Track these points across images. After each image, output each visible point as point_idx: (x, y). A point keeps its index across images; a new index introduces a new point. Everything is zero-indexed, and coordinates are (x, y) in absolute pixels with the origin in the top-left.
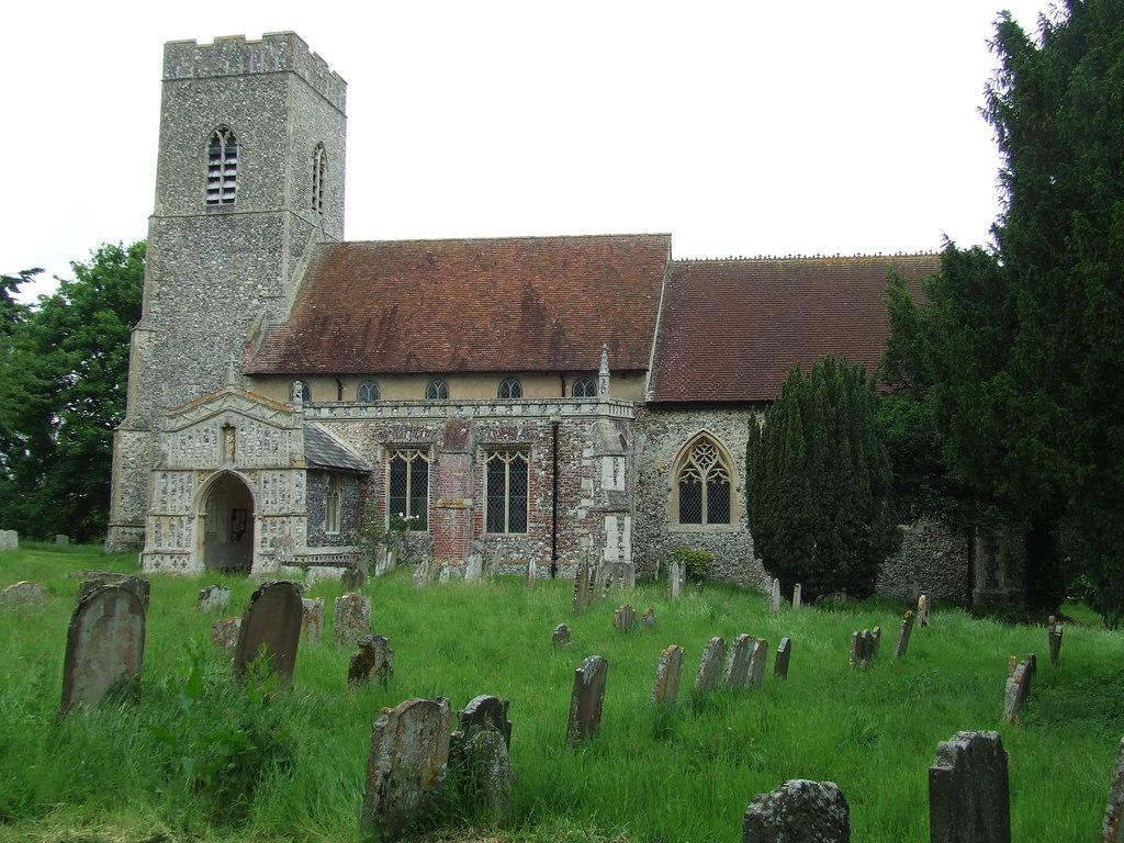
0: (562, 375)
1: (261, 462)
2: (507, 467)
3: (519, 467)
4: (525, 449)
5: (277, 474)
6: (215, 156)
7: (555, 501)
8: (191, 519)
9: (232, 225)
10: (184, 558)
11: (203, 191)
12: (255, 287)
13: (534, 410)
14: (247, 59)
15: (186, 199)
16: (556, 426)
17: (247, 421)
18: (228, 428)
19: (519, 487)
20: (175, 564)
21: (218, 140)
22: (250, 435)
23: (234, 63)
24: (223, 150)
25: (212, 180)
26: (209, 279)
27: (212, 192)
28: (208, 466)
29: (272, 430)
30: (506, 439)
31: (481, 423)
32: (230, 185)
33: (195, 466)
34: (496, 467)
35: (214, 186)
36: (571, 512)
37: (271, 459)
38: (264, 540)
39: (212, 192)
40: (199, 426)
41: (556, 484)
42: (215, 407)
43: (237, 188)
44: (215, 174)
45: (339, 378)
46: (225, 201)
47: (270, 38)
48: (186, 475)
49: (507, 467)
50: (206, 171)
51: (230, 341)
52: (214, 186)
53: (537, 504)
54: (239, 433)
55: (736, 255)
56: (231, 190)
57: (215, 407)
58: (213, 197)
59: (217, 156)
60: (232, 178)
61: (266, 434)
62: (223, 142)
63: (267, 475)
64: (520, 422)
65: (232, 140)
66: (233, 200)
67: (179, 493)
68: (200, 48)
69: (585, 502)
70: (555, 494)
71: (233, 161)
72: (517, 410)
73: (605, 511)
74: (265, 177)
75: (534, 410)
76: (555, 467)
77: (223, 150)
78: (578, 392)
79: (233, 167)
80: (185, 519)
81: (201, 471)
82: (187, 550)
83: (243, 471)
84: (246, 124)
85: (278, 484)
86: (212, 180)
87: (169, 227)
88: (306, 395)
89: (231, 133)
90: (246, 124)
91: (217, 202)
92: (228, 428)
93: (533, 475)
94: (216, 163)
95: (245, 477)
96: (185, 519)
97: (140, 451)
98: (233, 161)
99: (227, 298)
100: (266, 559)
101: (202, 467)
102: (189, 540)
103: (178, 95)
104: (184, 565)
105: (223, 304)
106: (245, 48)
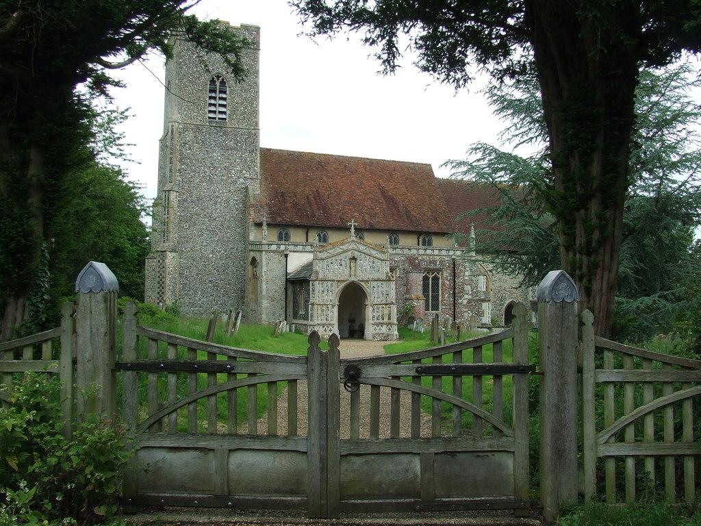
0: (419, 234)
1: (371, 276)
2: (430, 279)
3: (436, 279)
5: (379, 283)
7: (454, 297)
8: (333, 306)
9: (225, 134)
12: (241, 171)
15: (196, 114)
18: (354, 259)
19: (435, 290)
21: (215, 82)
22: (364, 263)
24: (218, 88)
25: (210, 105)
26: (212, 164)
27: (210, 112)
29: (376, 260)
30: (432, 266)
31: (420, 258)
32: (223, 109)
33: (335, 278)
34: (425, 279)
35: (213, 108)
36: (460, 301)
37: (376, 276)
39: (210, 112)
40: (336, 257)
41: (455, 288)
42: (345, 247)
43: (228, 112)
45: (307, 228)
46: (219, 119)
47: (245, 28)
48: (329, 283)
49: (430, 279)
50: (207, 99)
51: (227, 201)
52: (213, 108)
53: (445, 297)
54: (358, 261)
56: (225, 113)
57: (345, 247)
58: (212, 115)
59: (215, 91)
62: (218, 84)
63: (375, 284)
64: (438, 258)
65: (223, 83)
66: (225, 119)
69: (466, 296)
70: (454, 293)
71: (224, 96)
72: (429, 252)
73: (484, 301)
74: (245, 108)
75: (444, 253)
76: (454, 282)
77: (218, 88)
78: (424, 244)
79: (225, 99)
80: (330, 307)
81: (338, 281)
82: (332, 322)
83: (362, 281)
85: (380, 289)
86: (210, 105)
87: (185, 130)
89: (223, 79)
91: (215, 118)
92: (354, 259)
94: (213, 95)
95: (362, 283)
96: (330, 307)
98: (224, 96)
99: (224, 176)
100: (375, 326)
101: (339, 279)
102: (332, 317)
105: (222, 180)
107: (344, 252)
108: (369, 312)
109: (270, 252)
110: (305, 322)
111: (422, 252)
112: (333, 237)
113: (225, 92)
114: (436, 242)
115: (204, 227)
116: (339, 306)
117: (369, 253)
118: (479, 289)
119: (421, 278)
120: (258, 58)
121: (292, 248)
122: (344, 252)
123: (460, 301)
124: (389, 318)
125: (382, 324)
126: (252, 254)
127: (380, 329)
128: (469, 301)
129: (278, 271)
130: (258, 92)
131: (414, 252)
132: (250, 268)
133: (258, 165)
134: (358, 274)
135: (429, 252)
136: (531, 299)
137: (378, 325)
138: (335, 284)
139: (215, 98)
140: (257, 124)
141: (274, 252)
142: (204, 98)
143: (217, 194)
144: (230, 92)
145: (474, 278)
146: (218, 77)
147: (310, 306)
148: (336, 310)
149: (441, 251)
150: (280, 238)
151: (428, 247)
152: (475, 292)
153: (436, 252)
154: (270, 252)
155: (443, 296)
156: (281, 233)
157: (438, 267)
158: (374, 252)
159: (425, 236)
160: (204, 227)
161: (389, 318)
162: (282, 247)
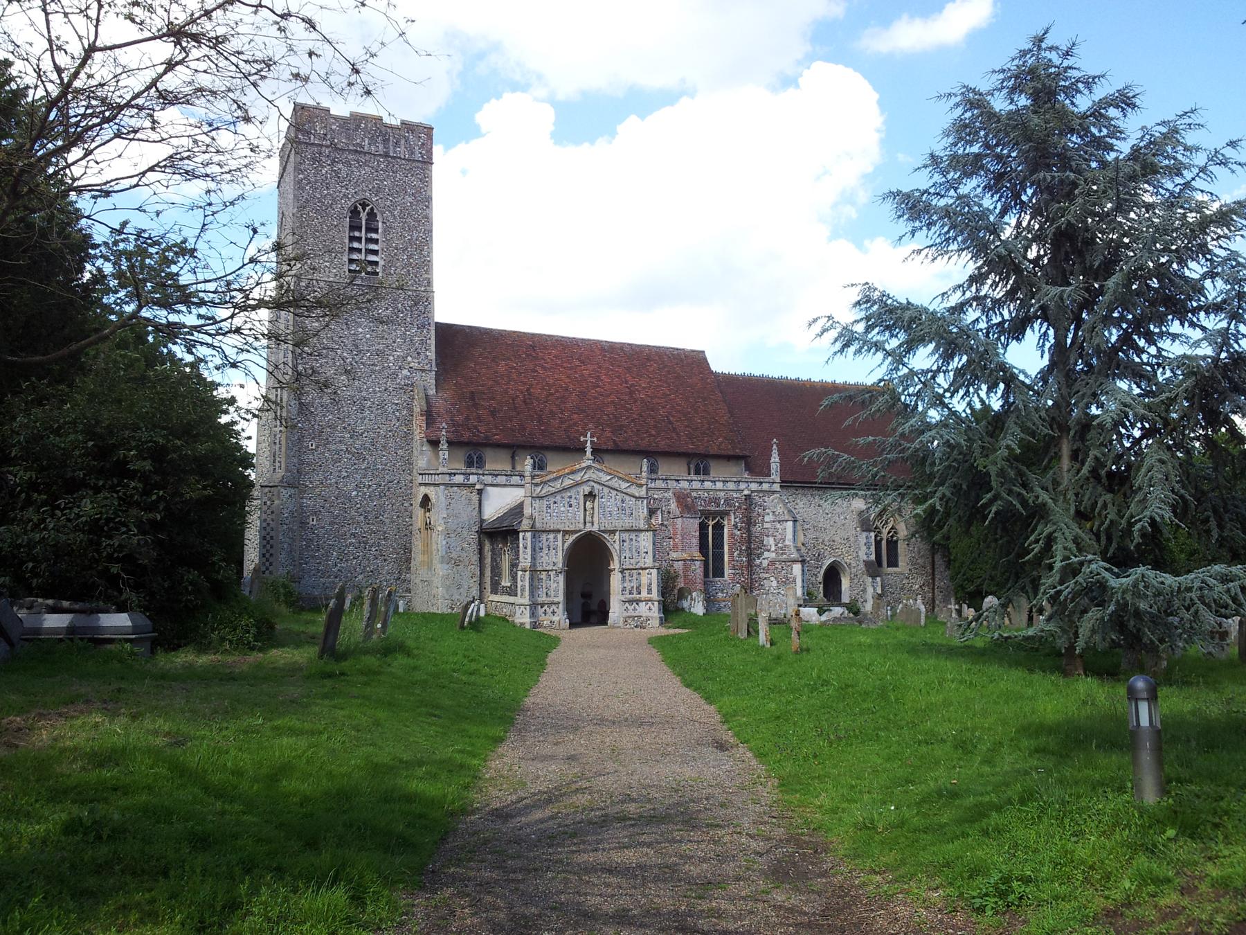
0: (686, 456)
1: (619, 524)
3: (719, 528)
4: (724, 514)
5: (633, 536)
6: (354, 227)
10: (554, 607)
11: (346, 259)
12: (404, 358)
13: (731, 486)
14: (386, 141)
16: (748, 497)
17: (606, 490)
18: (591, 496)
19: (718, 544)
20: (545, 613)
22: (609, 502)
23: (373, 141)
25: (352, 250)
28: (572, 528)
30: (713, 508)
31: (694, 494)
33: (561, 527)
34: (703, 527)
36: (758, 562)
37: (628, 522)
38: (624, 589)
41: (749, 542)
42: (578, 477)
43: (381, 263)
44: (356, 245)
45: (514, 449)
47: (408, 126)
48: (551, 536)
50: (347, 241)
55: (747, 372)
57: (578, 477)
60: (375, 252)
61: (623, 501)
62: (363, 216)
63: (626, 536)
64: (722, 494)
65: (372, 215)
67: (545, 551)
68: (336, 118)
69: (766, 554)
70: (749, 548)
71: (374, 236)
72: (708, 485)
73: (794, 561)
74: (410, 257)
75: (731, 486)
76: (749, 531)
78: (697, 473)
79: (376, 241)
81: (566, 532)
82: (556, 600)
84: (388, 203)
86: (352, 250)
88: (653, 470)
89: (372, 209)
90: (388, 203)
93: (732, 536)
94: (357, 234)
97: (291, 507)
98: (374, 236)
102: (556, 591)
103: (314, 159)
104: (554, 613)
105: (373, 371)
106: (383, 129)
107: (578, 484)
108: (615, 581)
109: (452, 485)
110: (512, 599)
111: (696, 485)
112: (555, 464)
113: (376, 231)
114: (717, 470)
115: (344, 447)
116: (567, 572)
117: (616, 486)
118: (787, 543)
119: (697, 526)
120: (430, 177)
121: (488, 479)
122: (578, 484)
123: (758, 562)
124: (649, 591)
125: (638, 601)
126: (423, 490)
127: (635, 609)
128: (772, 563)
129: (467, 515)
130: (431, 231)
131: (684, 485)
132: (419, 512)
133: (433, 348)
134: (596, 519)
135: (708, 485)
136: (865, 558)
137: (631, 602)
138: (560, 536)
139: (359, 240)
140: (429, 283)
141: (459, 486)
142: (341, 238)
143: (364, 394)
144: (385, 231)
145: (778, 526)
146: (364, 206)
147: (520, 573)
148: (561, 578)
149: (724, 484)
150: (469, 464)
151: (706, 477)
152: (782, 550)
153: (719, 485)
154: (452, 485)
155: (731, 554)
156: (470, 457)
157: (722, 508)
158: (624, 485)
159: (700, 463)
160: (344, 447)
161: (649, 591)
162: (473, 479)
